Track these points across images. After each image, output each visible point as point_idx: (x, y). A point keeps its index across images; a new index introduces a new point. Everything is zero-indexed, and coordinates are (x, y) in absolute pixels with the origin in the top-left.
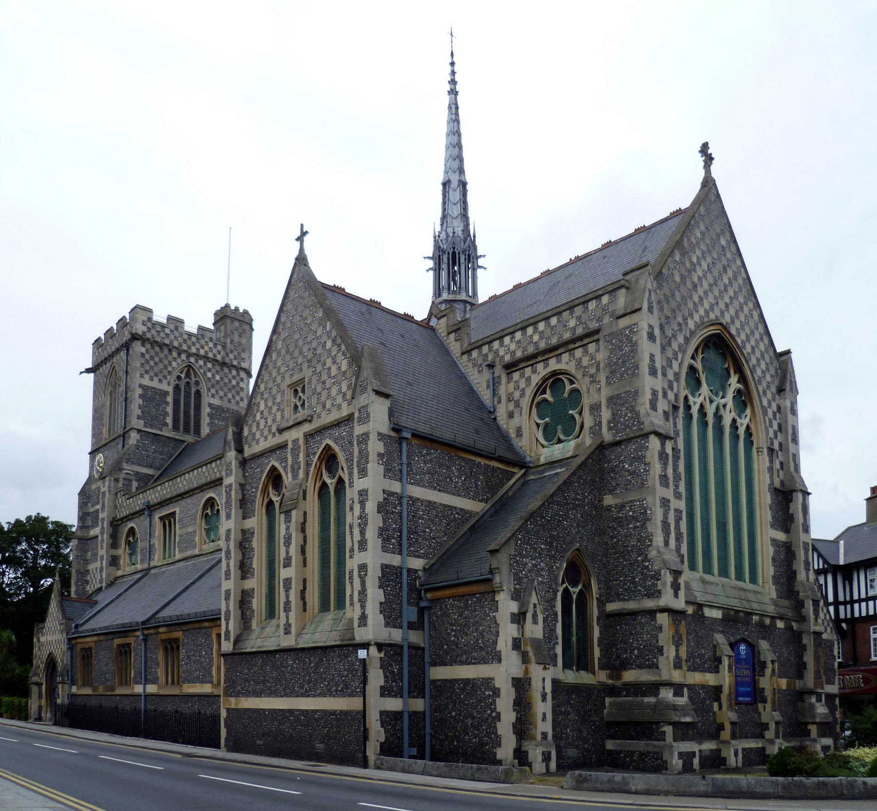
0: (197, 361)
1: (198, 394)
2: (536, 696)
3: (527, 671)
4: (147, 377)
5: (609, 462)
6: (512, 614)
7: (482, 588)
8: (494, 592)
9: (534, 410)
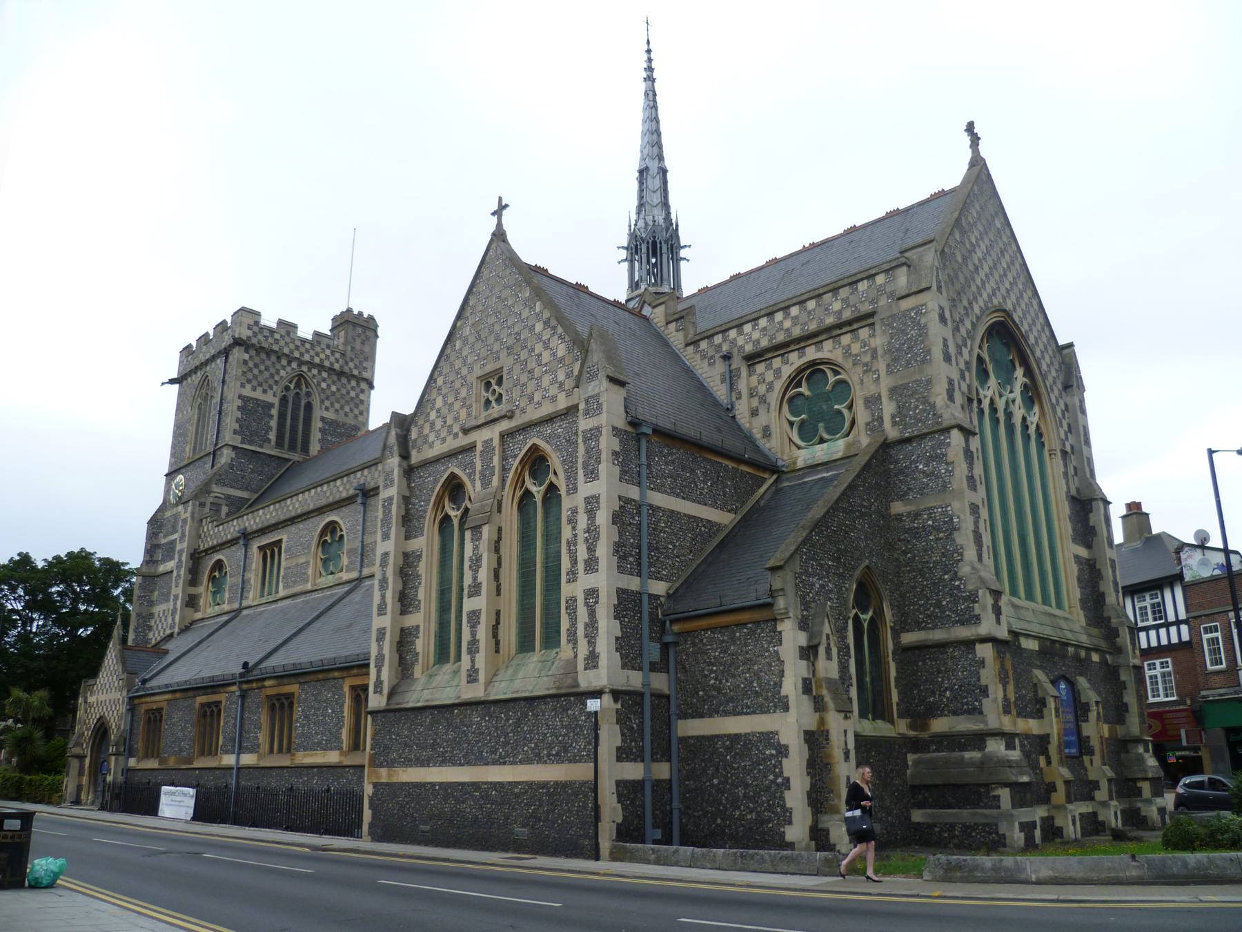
0: (310, 370)
1: (309, 407)
2: (837, 753)
3: (822, 721)
4: (248, 386)
5: (896, 462)
6: (801, 648)
7: (764, 614)
8: (775, 620)
9: (785, 407)
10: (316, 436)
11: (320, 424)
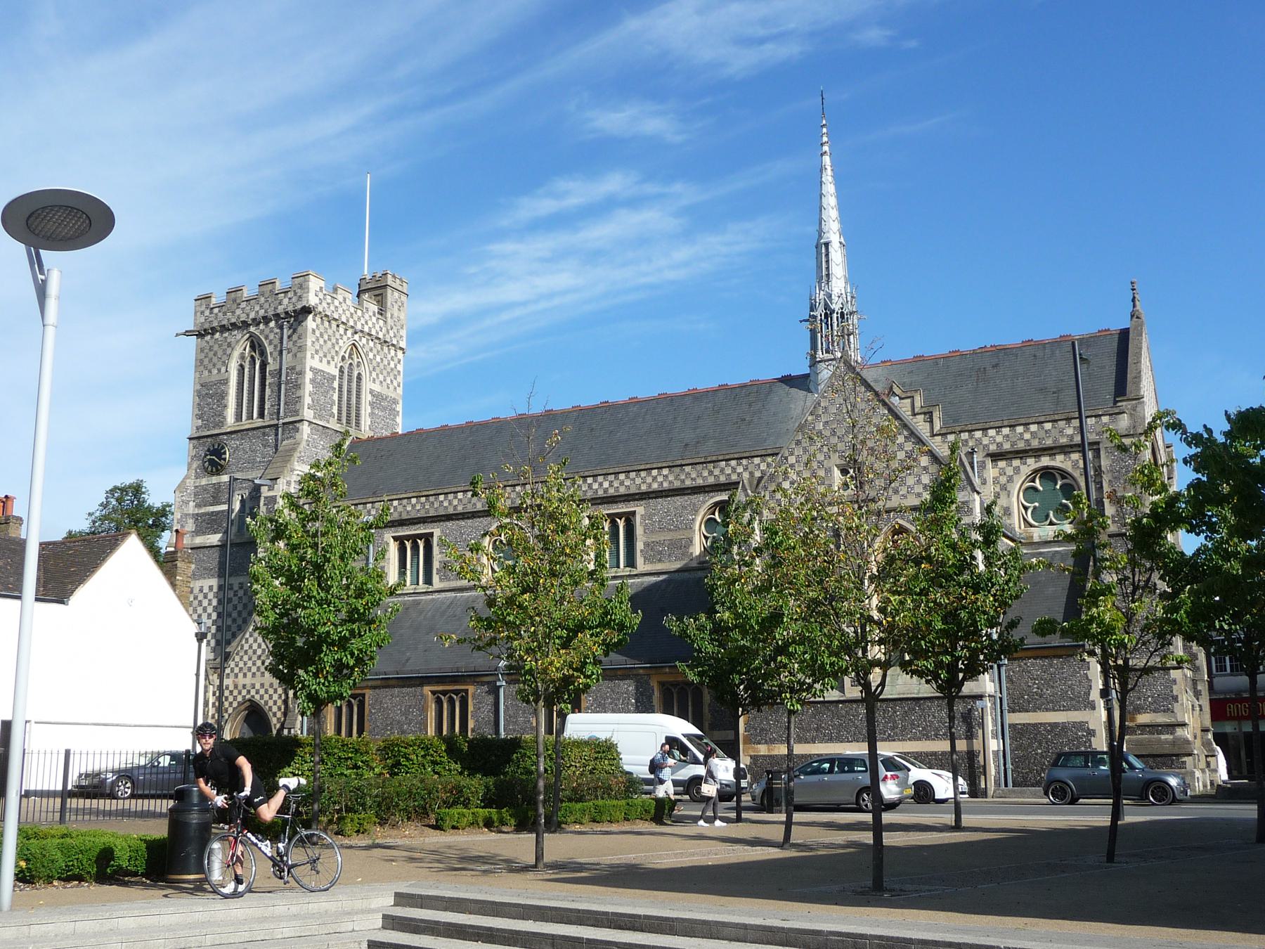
1: (359, 378)
10: (366, 410)
11: (369, 397)
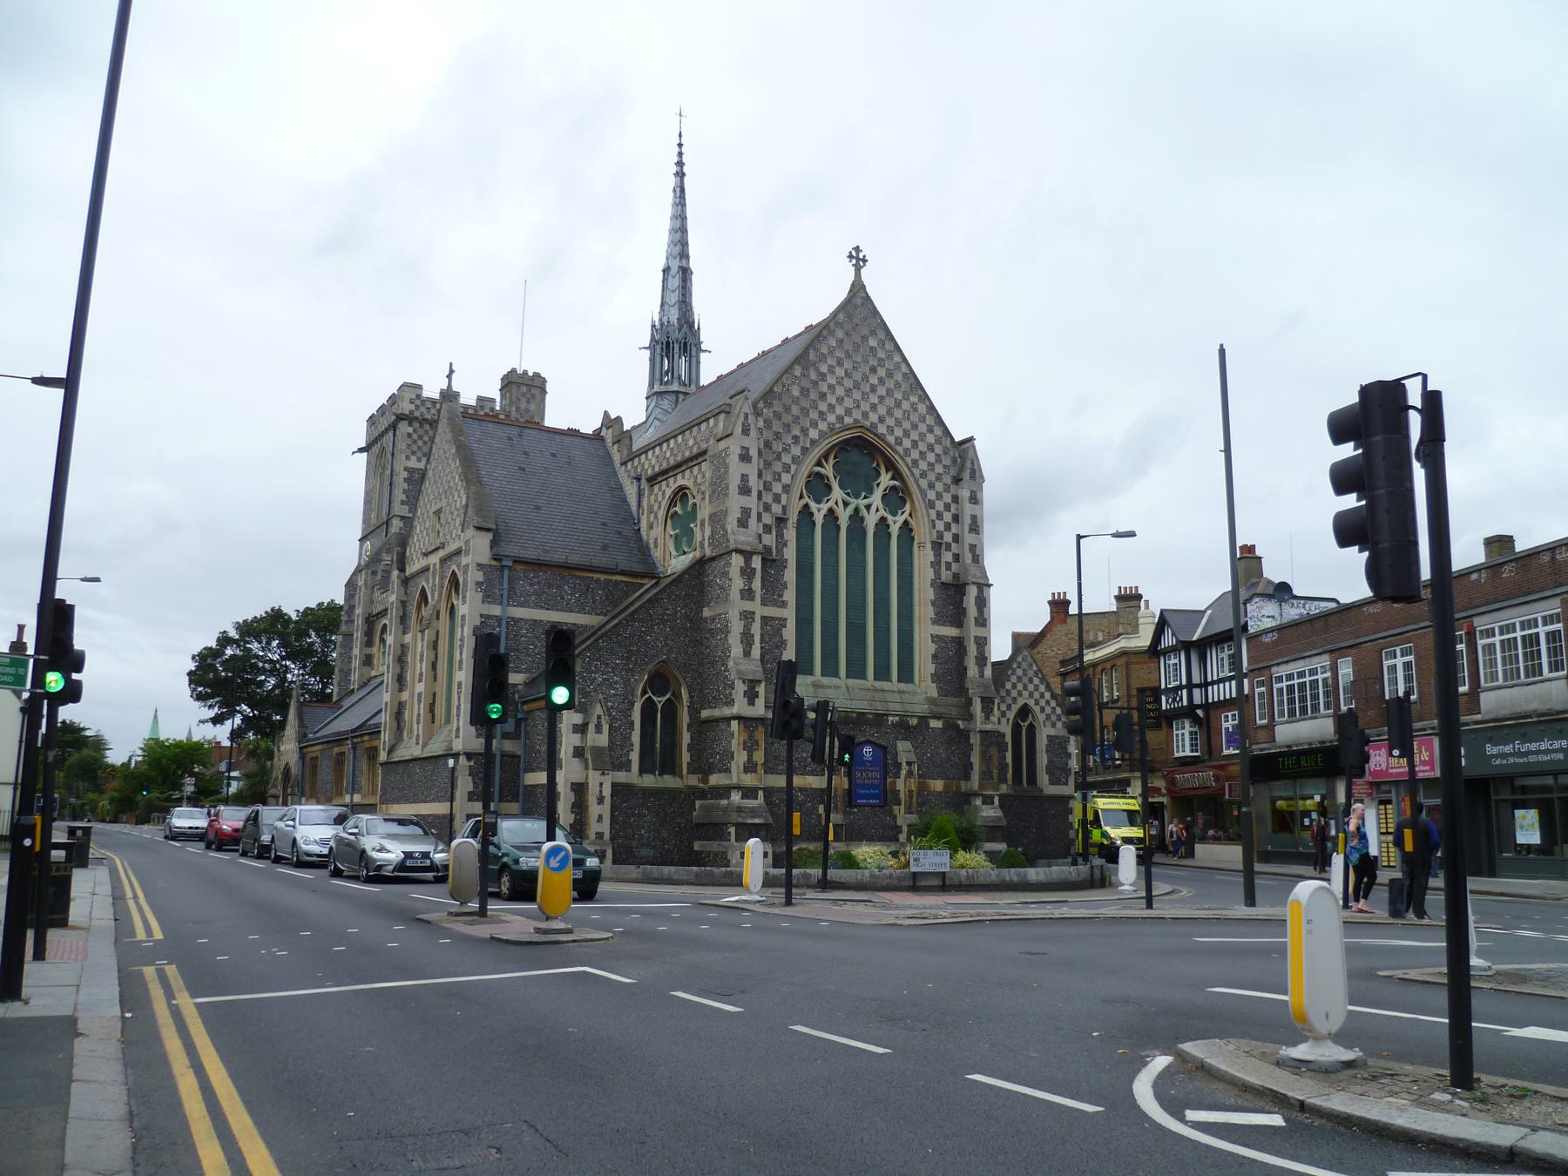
4: (414, 458)
